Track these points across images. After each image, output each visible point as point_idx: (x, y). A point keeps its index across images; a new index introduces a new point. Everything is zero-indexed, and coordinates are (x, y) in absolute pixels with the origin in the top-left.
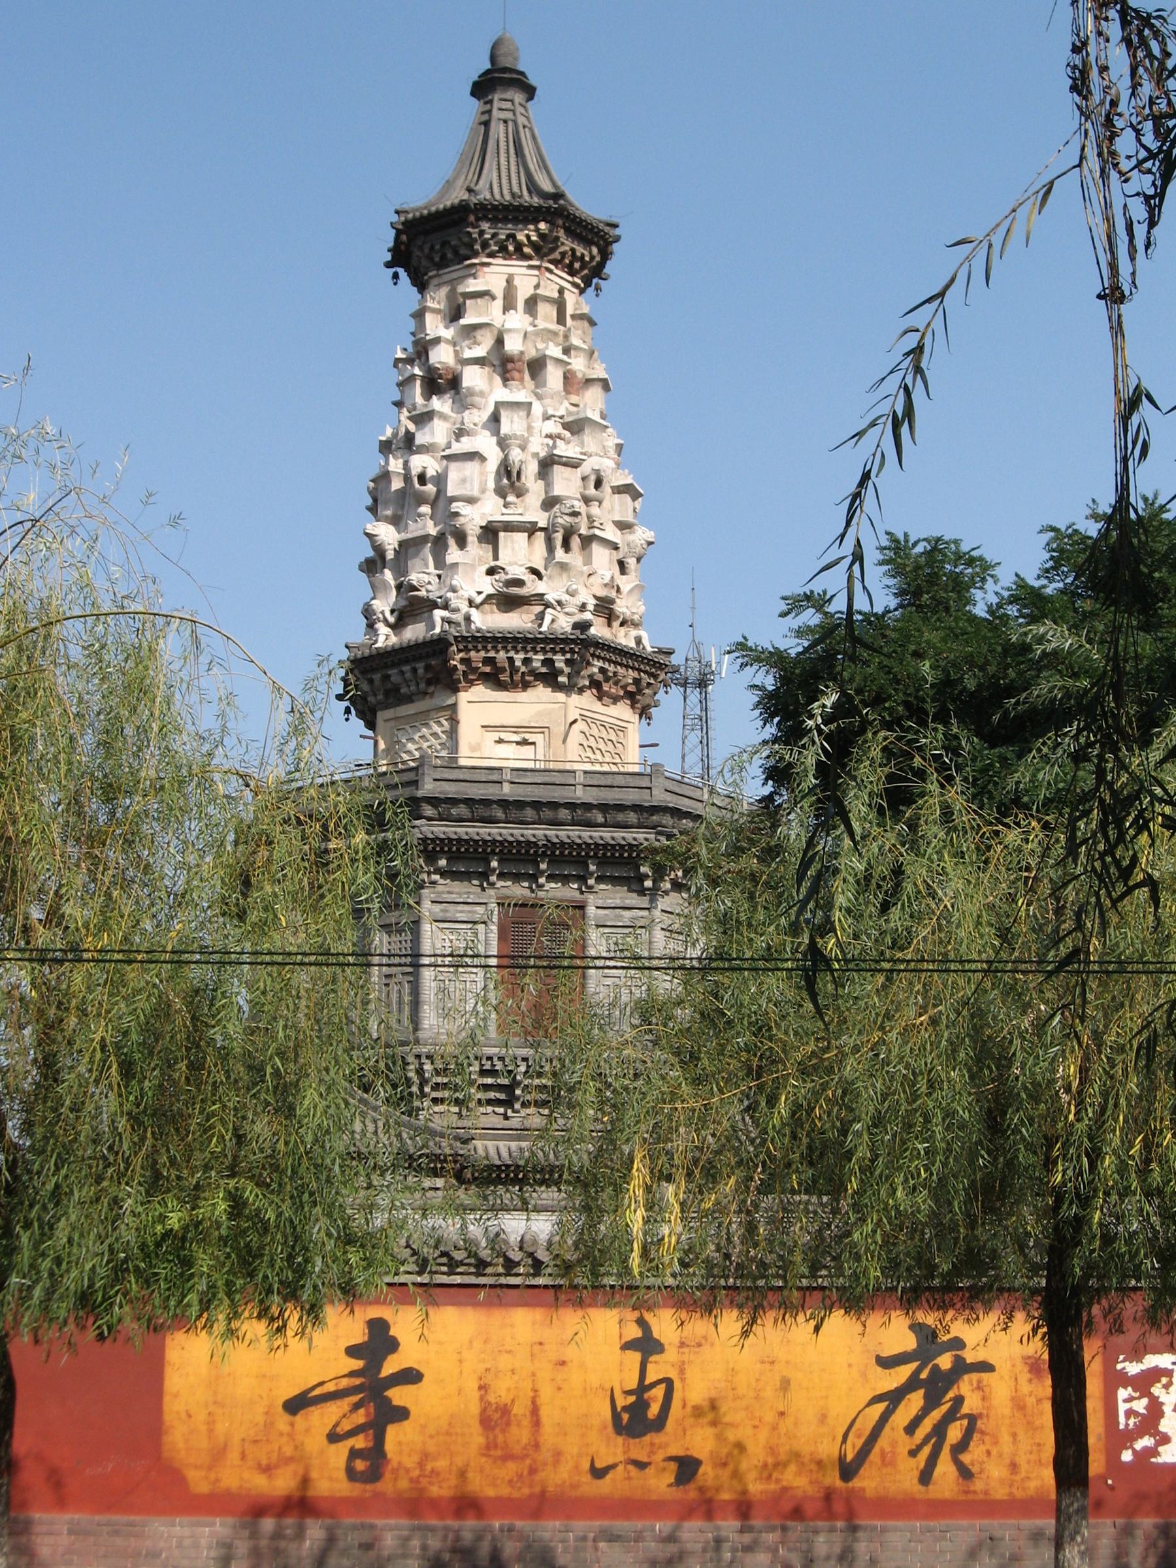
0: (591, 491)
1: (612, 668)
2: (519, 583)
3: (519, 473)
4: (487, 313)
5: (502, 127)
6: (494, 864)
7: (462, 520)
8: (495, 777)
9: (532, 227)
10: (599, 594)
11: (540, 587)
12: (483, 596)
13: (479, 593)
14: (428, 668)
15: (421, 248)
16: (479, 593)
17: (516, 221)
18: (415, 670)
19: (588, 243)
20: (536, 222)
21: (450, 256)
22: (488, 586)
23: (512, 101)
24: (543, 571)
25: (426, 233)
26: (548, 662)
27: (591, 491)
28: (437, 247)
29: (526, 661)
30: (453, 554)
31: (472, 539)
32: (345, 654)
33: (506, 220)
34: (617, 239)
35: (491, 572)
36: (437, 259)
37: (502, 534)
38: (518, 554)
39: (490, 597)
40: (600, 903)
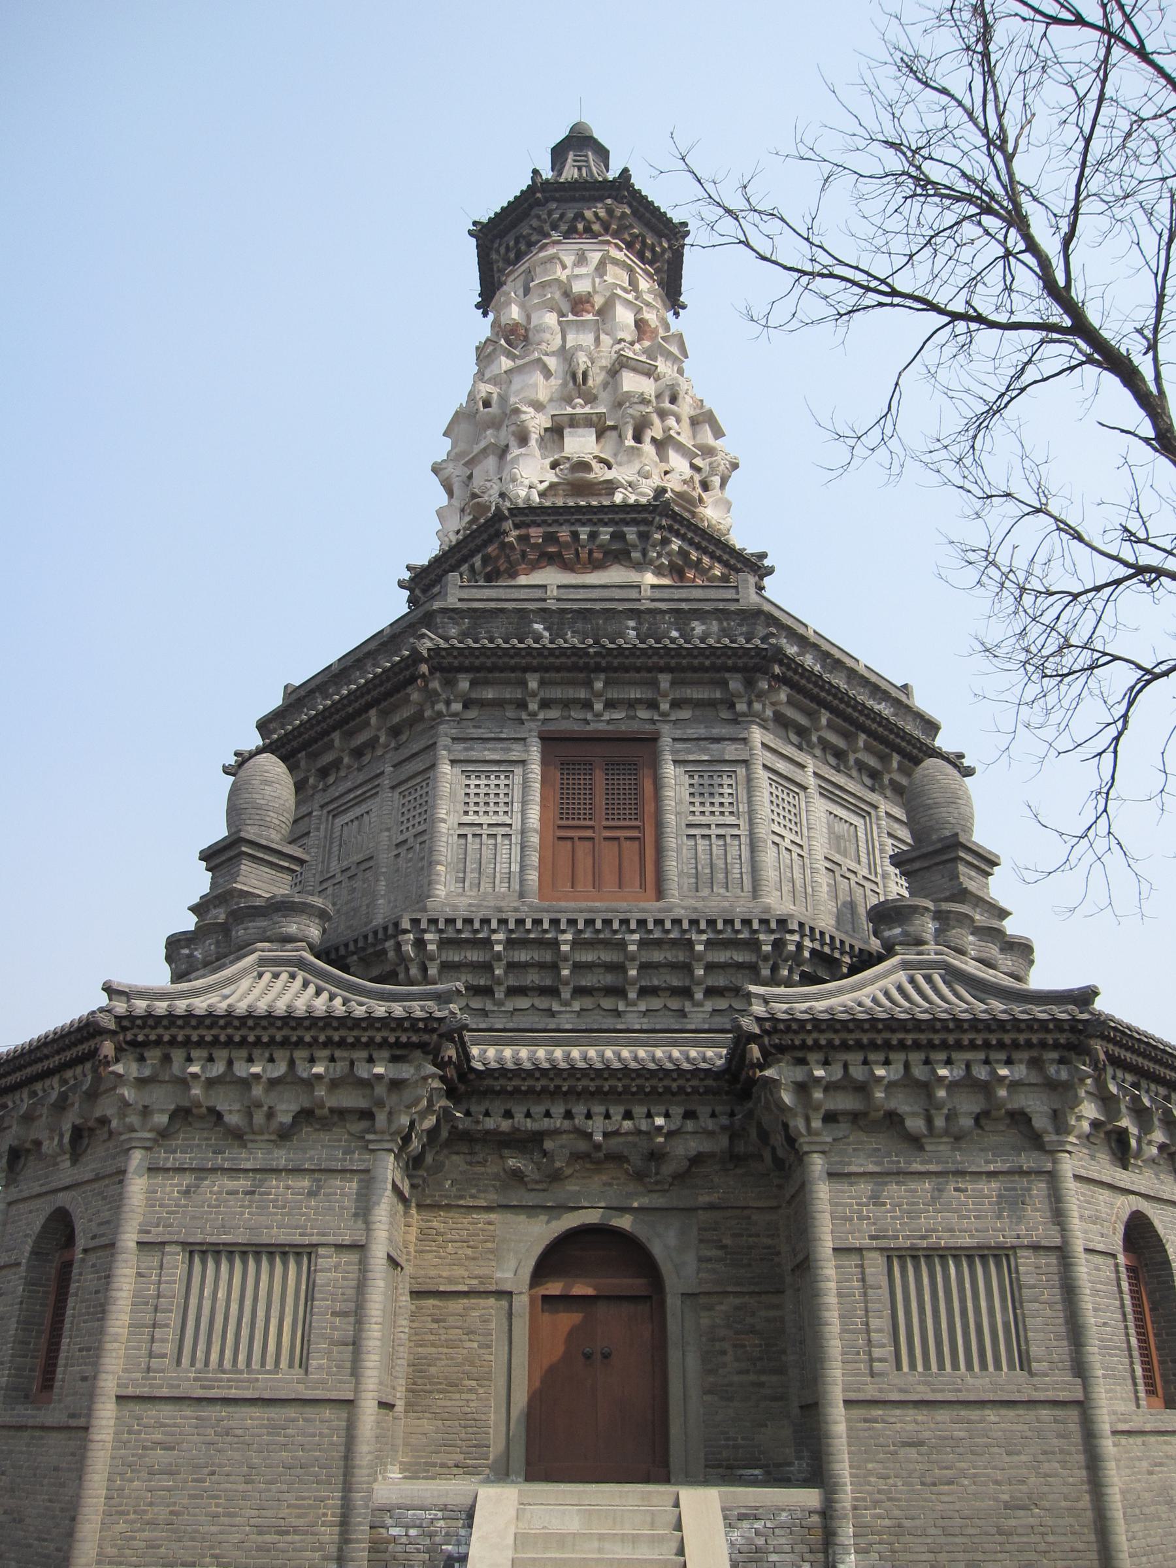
0: (667, 405)
1: (694, 555)
2: (584, 466)
3: (585, 374)
4: (555, 273)
5: (576, 170)
6: (533, 685)
7: (523, 417)
8: (538, 594)
9: (599, 205)
10: (677, 490)
11: (609, 475)
12: (546, 484)
13: (541, 482)
14: (486, 560)
15: (498, 251)
16: (541, 482)
17: (583, 199)
18: (472, 567)
19: (659, 235)
20: (601, 199)
21: (523, 247)
22: (551, 477)
23: (586, 156)
24: (612, 460)
25: (502, 235)
26: (618, 536)
27: (667, 405)
28: (512, 243)
29: (593, 536)
30: (515, 451)
31: (534, 438)
32: (407, 575)
33: (573, 199)
35: (554, 465)
36: (512, 255)
37: (567, 431)
38: (581, 444)
39: (552, 486)
40: (678, 733)
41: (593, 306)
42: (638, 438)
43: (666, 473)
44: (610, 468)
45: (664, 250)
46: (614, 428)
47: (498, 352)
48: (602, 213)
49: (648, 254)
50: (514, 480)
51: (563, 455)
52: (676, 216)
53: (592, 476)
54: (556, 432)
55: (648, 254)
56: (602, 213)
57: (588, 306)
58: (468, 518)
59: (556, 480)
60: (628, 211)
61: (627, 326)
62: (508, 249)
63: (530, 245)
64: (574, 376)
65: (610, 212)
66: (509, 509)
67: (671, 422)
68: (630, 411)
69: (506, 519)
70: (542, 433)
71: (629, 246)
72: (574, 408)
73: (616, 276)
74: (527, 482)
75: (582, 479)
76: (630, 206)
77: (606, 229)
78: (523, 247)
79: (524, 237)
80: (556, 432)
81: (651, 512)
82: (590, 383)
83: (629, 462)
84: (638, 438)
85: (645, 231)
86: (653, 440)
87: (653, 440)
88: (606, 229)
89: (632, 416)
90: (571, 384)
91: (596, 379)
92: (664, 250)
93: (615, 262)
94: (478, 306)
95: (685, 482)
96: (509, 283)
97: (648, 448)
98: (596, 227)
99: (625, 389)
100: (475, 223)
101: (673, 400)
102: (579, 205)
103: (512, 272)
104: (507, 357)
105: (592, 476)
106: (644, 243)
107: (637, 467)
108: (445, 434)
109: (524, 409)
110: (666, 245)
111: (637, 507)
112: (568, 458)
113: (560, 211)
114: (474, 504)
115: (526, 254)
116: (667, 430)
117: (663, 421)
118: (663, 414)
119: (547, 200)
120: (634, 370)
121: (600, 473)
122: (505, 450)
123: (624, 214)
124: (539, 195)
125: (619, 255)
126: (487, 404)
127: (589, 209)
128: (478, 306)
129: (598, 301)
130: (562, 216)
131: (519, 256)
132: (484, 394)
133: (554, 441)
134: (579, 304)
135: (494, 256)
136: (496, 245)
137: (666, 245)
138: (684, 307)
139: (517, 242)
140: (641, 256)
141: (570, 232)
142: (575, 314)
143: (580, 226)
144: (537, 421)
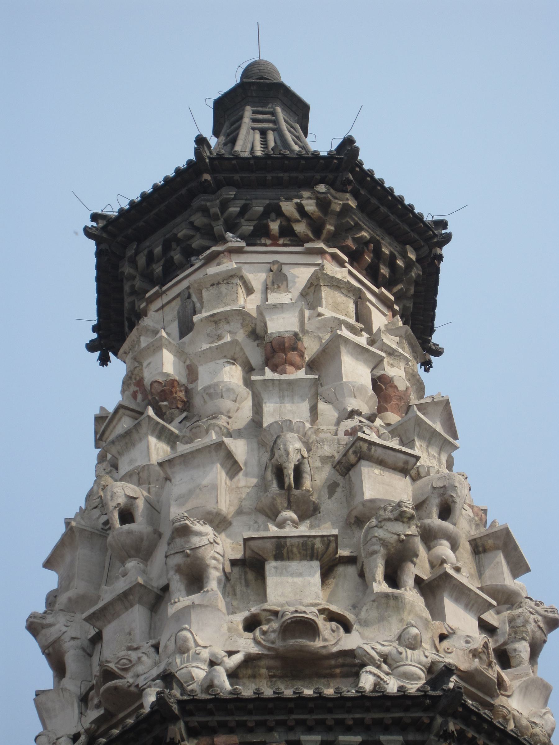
0: (435, 521)
3: (298, 471)
4: (236, 300)
5: (258, 136)
7: (196, 541)
9: (306, 194)
12: (238, 658)
15: (133, 262)
16: (230, 653)
17: (279, 184)
19: (402, 240)
20: (309, 185)
21: (177, 257)
22: (247, 645)
23: (273, 113)
24: (351, 617)
27: (435, 521)
28: (158, 250)
30: (181, 600)
31: (214, 577)
33: (263, 184)
34: (447, 238)
35: (251, 624)
36: (158, 269)
37: (271, 566)
39: (250, 660)
41: (302, 355)
42: (393, 579)
43: (443, 637)
44: (348, 628)
45: (409, 264)
46: (351, 560)
47: (144, 428)
48: (310, 206)
49: (384, 271)
50: (182, 650)
51: (267, 606)
52: (427, 208)
53: (318, 644)
54: (251, 567)
55: (384, 271)
56: (310, 206)
57: (293, 356)
58: (94, 714)
59: (255, 650)
60: (353, 203)
61: (361, 388)
62: (151, 259)
63: (190, 253)
64: (279, 473)
65: (323, 204)
66: (180, 703)
67: (444, 548)
68: (380, 533)
69: (174, 719)
70: (228, 569)
71: (355, 258)
72: (281, 525)
73: (336, 307)
74: (205, 654)
75: (302, 650)
76: (356, 195)
77: (317, 230)
78: (177, 257)
79: (178, 241)
80: (251, 567)
81: (426, 709)
82: (307, 484)
83: (382, 619)
84: (393, 579)
85: (379, 234)
86: (418, 581)
87: (418, 581)
88: (317, 230)
89: (384, 543)
90: (274, 486)
91: (316, 479)
92: (409, 264)
93: (336, 284)
94: (91, 347)
95: (475, 654)
96: (151, 313)
97: (411, 595)
98: (301, 228)
99: (368, 494)
100: (95, 217)
101: (446, 512)
102: (270, 193)
103: (157, 295)
104: (159, 437)
105: (318, 644)
106: (377, 253)
107: (395, 629)
108: (49, 564)
109: (198, 527)
110: (412, 256)
111: (402, 699)
112: (275, 613)
113: (242, 202)
114: (108, 693)
115: (182, 267)
116: (437, 563)
117: (429, 548)
118: (429, 537)
119: (219, 185)
120: (382, 463)
121: (331, 640)
122: (158, 598)
123: (346, 209)
124: (207, 177)
125: (341, 273)
126: (127, 516)
127: (289, 199)
128: (91, 347)
129: (311, 347)
130: (244, 209)
131: (170, 271)
132: (121, 500)
133: (247, 585)
134: (277, 352)
135: (127, 269)
136: (130, 252)
137: (412, 256)
138: (438, 352)
139: (167, 248)
140: (373, 274)
141: (257, 235)
142: (274, 369)
143: (274, 226)
144: (219, 549)
